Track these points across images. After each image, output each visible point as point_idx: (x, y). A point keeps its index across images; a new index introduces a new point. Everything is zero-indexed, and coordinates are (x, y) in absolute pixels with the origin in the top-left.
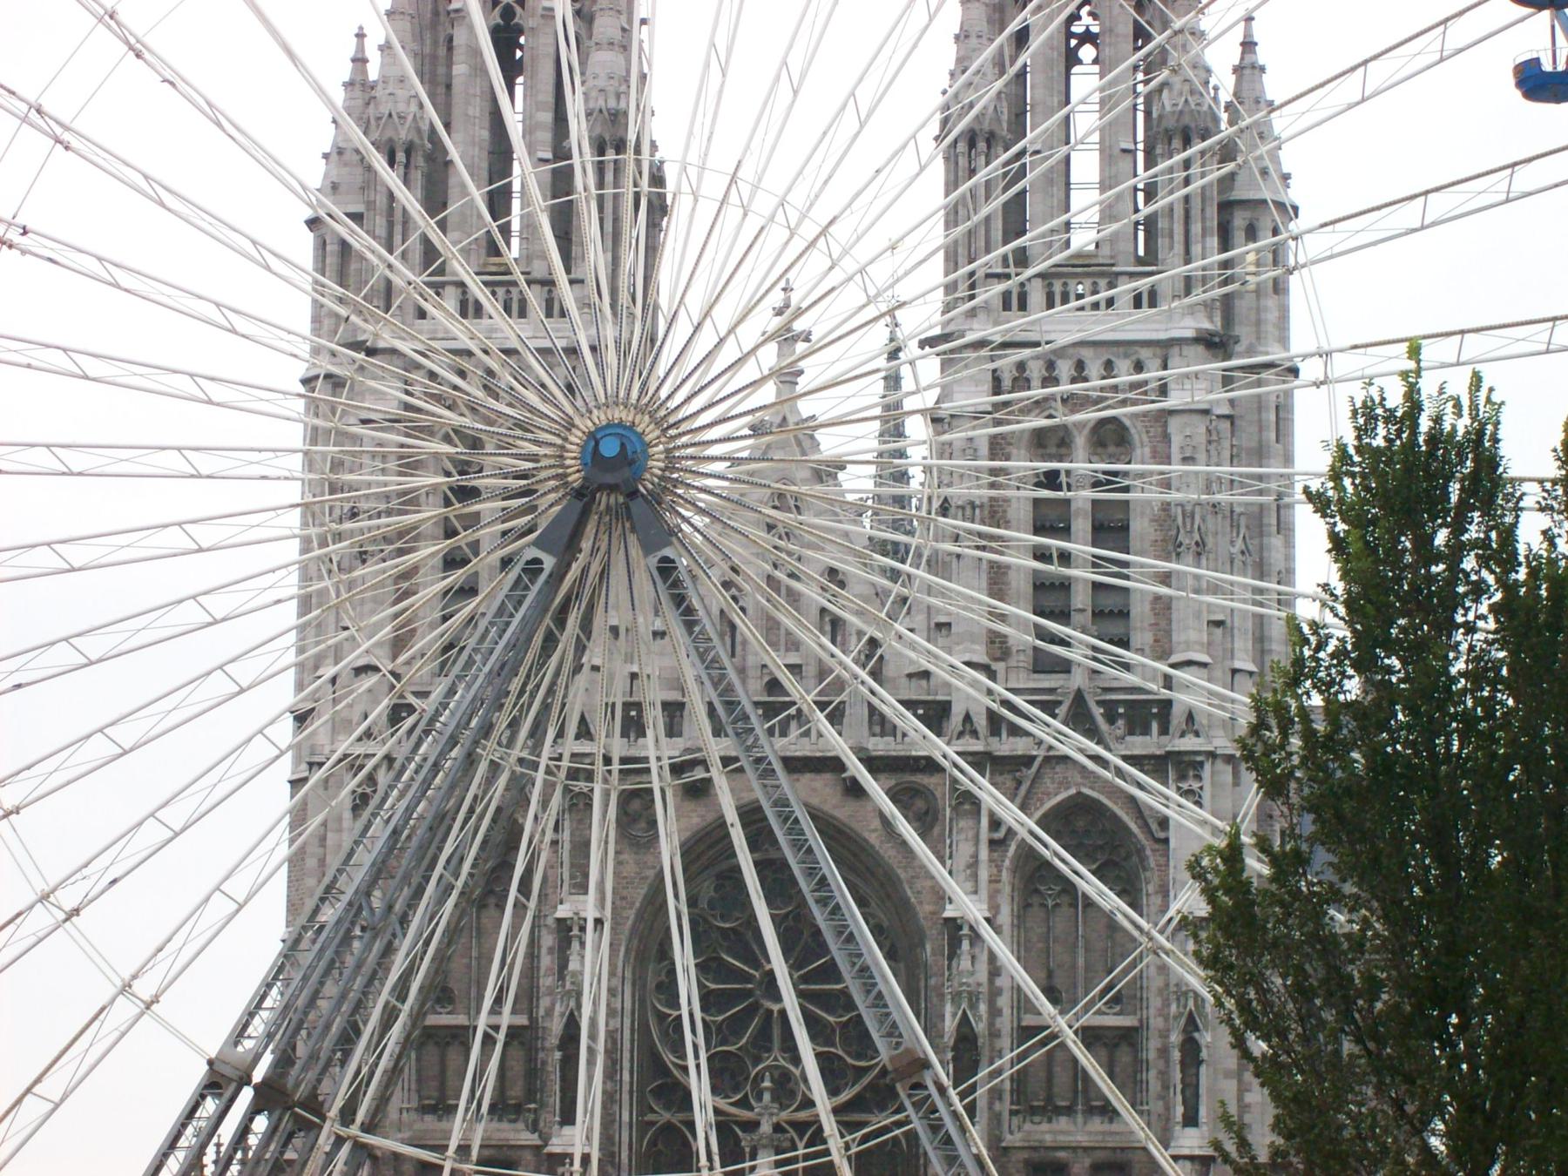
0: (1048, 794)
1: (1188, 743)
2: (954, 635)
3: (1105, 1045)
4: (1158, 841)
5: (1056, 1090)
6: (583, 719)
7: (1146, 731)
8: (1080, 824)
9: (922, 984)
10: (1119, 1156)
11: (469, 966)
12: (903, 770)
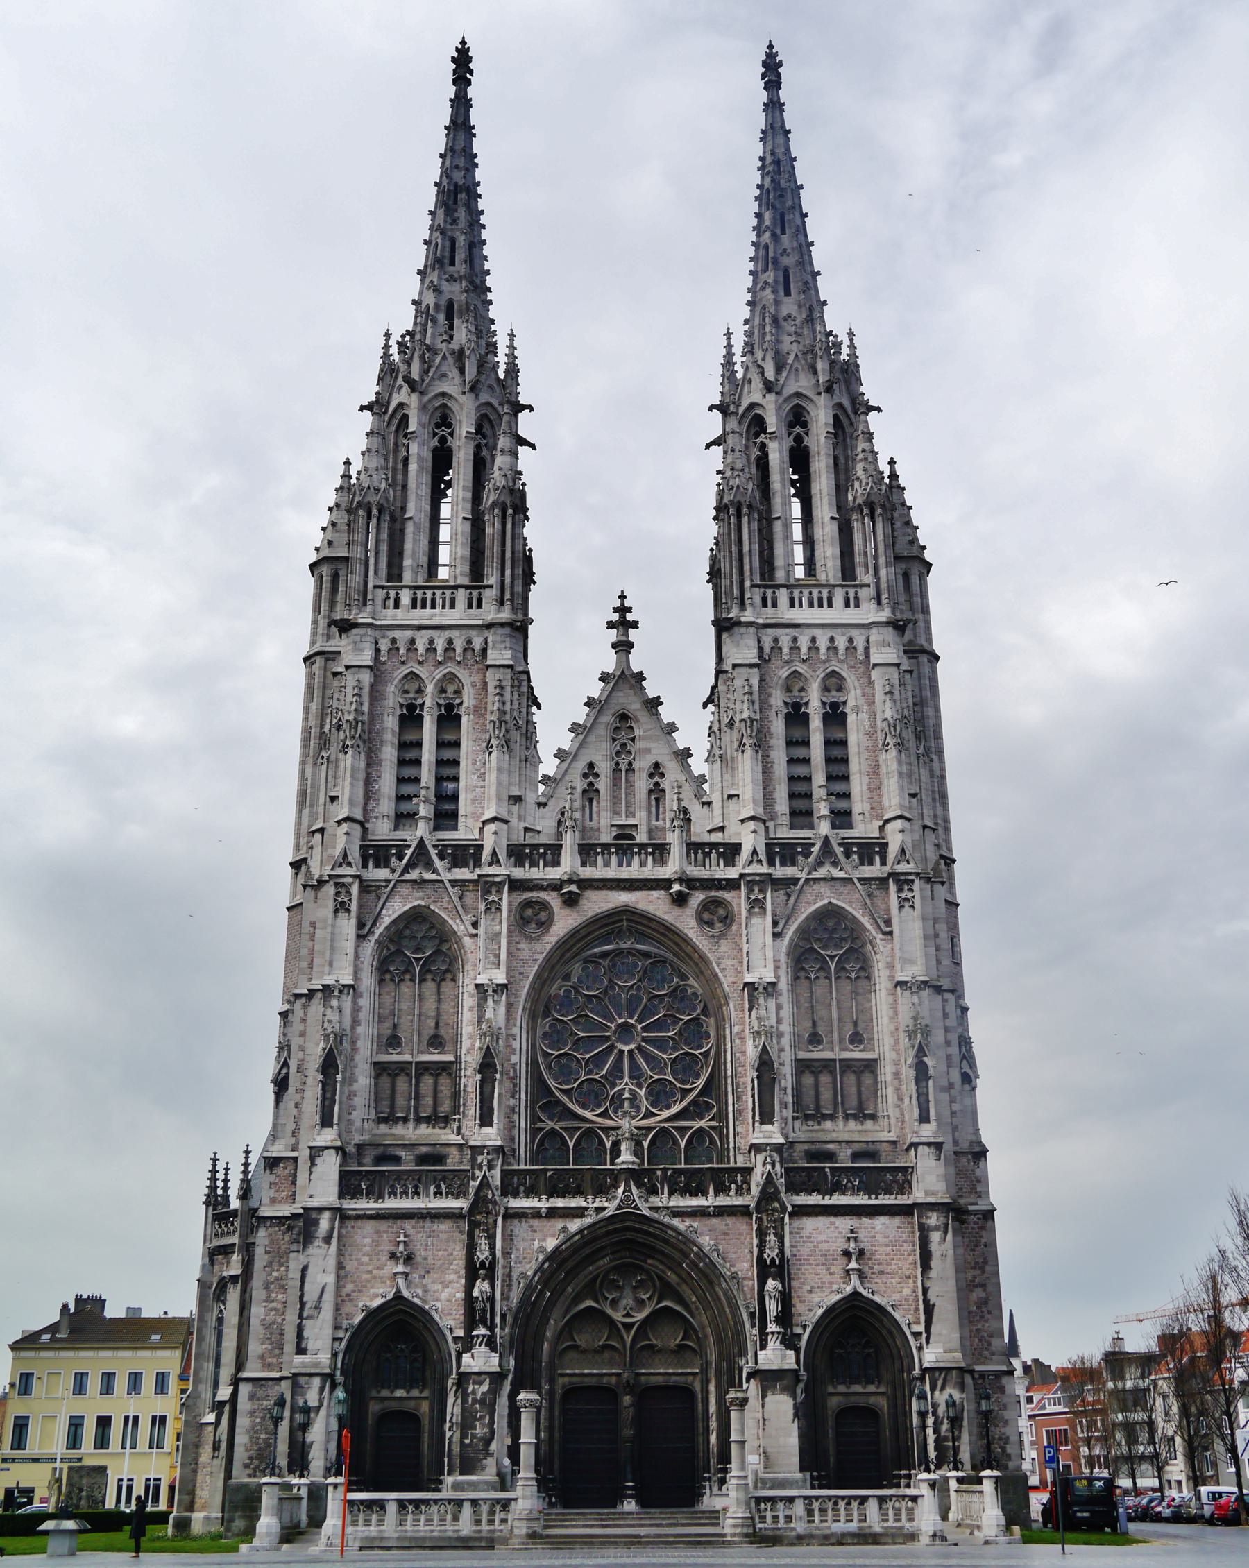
0: (809, 903)
1: (902, 868)
2: (735, 804)
3: (854, 1072)
4: (885, 933)
5: (822, 1103)
6: (494, 853)
7: (871, 863)
8: (830, 923)
9: (728, 1031)
11: (412, 1021)
12: (710, 889)
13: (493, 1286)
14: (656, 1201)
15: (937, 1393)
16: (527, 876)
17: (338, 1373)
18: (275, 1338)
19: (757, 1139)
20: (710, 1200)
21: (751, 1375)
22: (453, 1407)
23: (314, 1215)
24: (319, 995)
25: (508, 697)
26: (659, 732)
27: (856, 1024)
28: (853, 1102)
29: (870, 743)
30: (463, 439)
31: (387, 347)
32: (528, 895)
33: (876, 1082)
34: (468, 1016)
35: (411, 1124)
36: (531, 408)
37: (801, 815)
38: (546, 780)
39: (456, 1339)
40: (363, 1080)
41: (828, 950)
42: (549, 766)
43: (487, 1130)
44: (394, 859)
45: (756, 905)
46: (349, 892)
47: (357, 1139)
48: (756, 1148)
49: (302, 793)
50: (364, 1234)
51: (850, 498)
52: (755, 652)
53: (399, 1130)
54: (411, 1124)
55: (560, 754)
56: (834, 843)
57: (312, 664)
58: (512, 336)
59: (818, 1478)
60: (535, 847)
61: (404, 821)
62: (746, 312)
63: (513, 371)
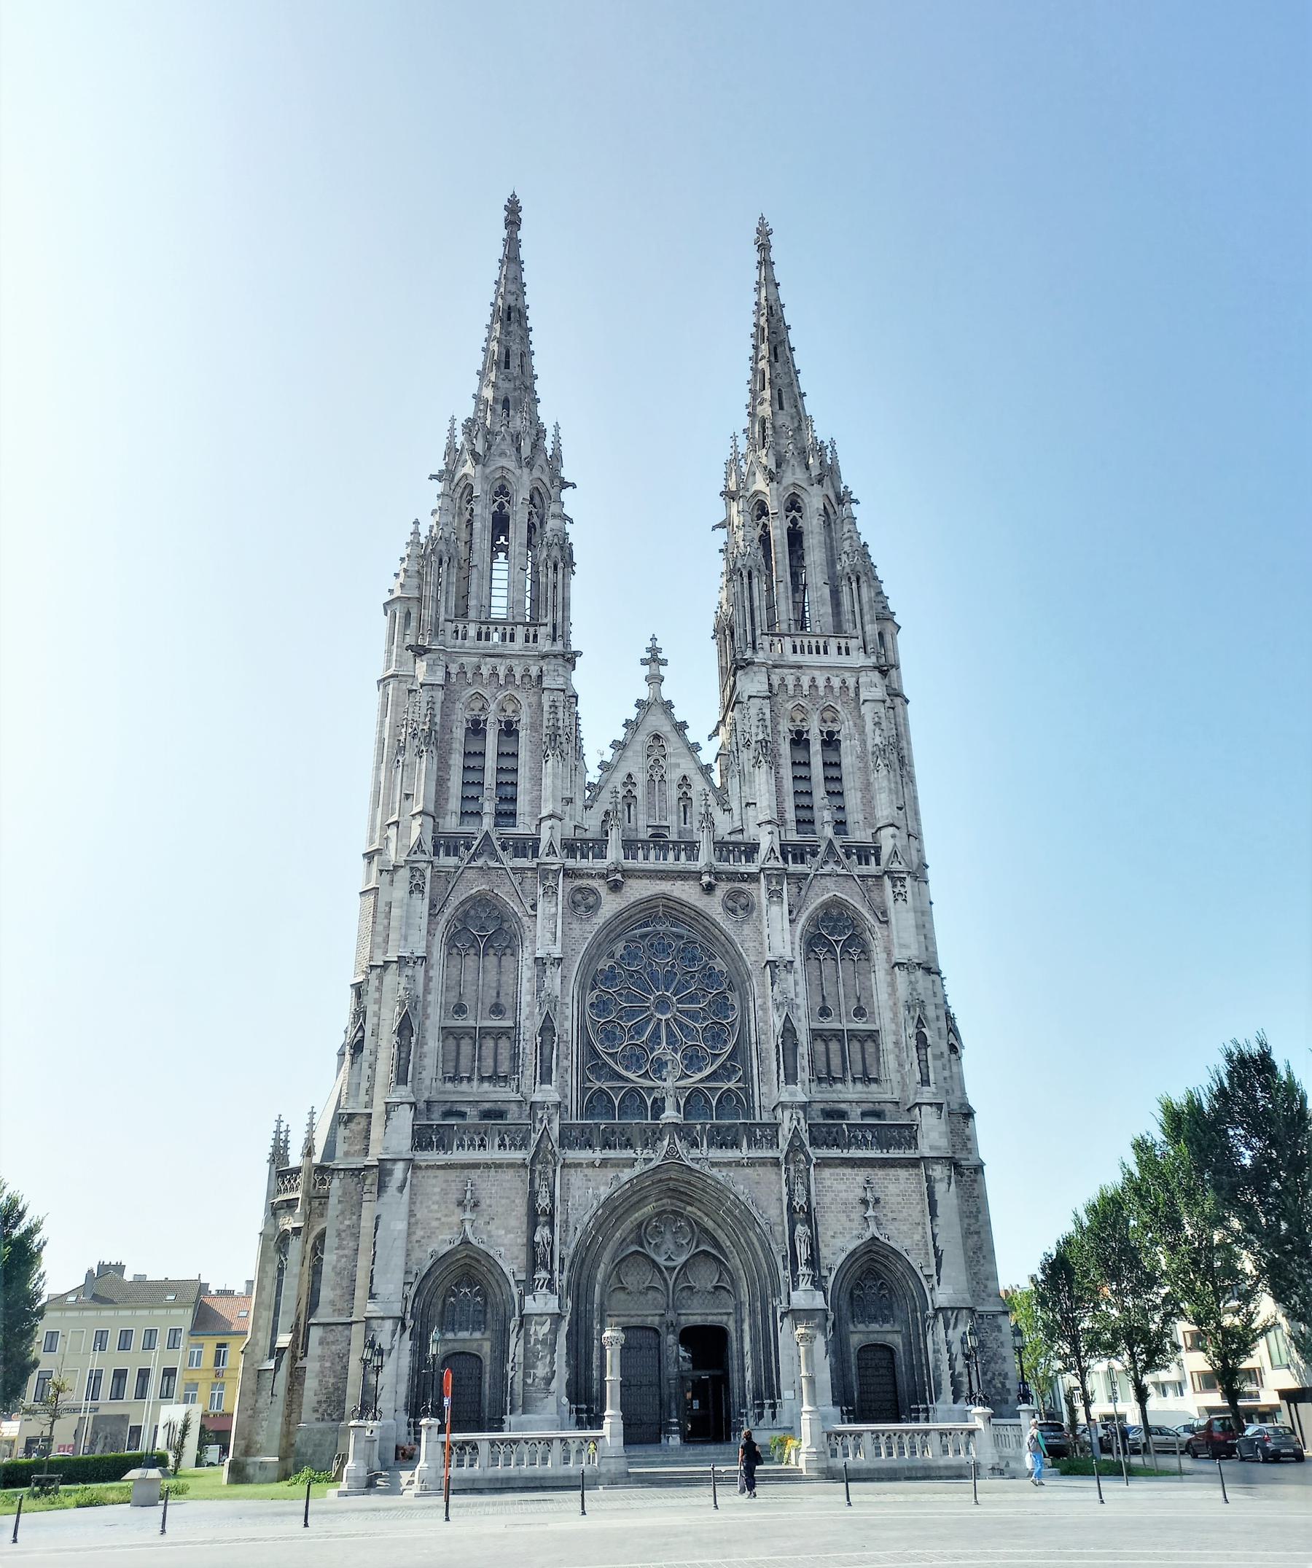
1: (896, 866)
7: (867, 864)
9: (751, 1004)
10: (877, 1107)
13: (552, 1232)
14: (695, 1153)
15: (950, 1331)
16: (578, 865)
17: (408, 1316)
18: (345, 1283)
19: (785, 1098)
20: (744, 1152)
21: (784, 1315)
22: (516, 1348)
23: (389, 1165)
24: (394, 966)
25: (560, 715)
26: (686, 751)
27: (859, 999)
28: (859, 1067)
29: (861, 765)
30: (520, 505)
31: (452, 429)
32: (578, 882)
33: (878, 1049)
34: (526, 987)
35: (475, 1083)
36: (574, 486)
37: (805, 823)
38: (591, 786)
39: (518, 1282)
40: (433, 1043)
41: (835, 936)
42: (593, 775)
43: (547, 1087)
44: (462, 849)
45: (774, 894)
46: (423, 876)
47: (426, 1096)
48: (783, 1105)
49: (377, 793)
50: (435, 1184)
51: (839, 567)
52: (767, 687)
53: (464, 1086)
54: (475, 1083)
55: (604, 766)
56: (837, 844)
57: (385, 686)
58: (557, 427)
59: (848, 1412)
60: (585, 841)
61: (467, 819)
62: (746, 422)
63: (557, 457)
